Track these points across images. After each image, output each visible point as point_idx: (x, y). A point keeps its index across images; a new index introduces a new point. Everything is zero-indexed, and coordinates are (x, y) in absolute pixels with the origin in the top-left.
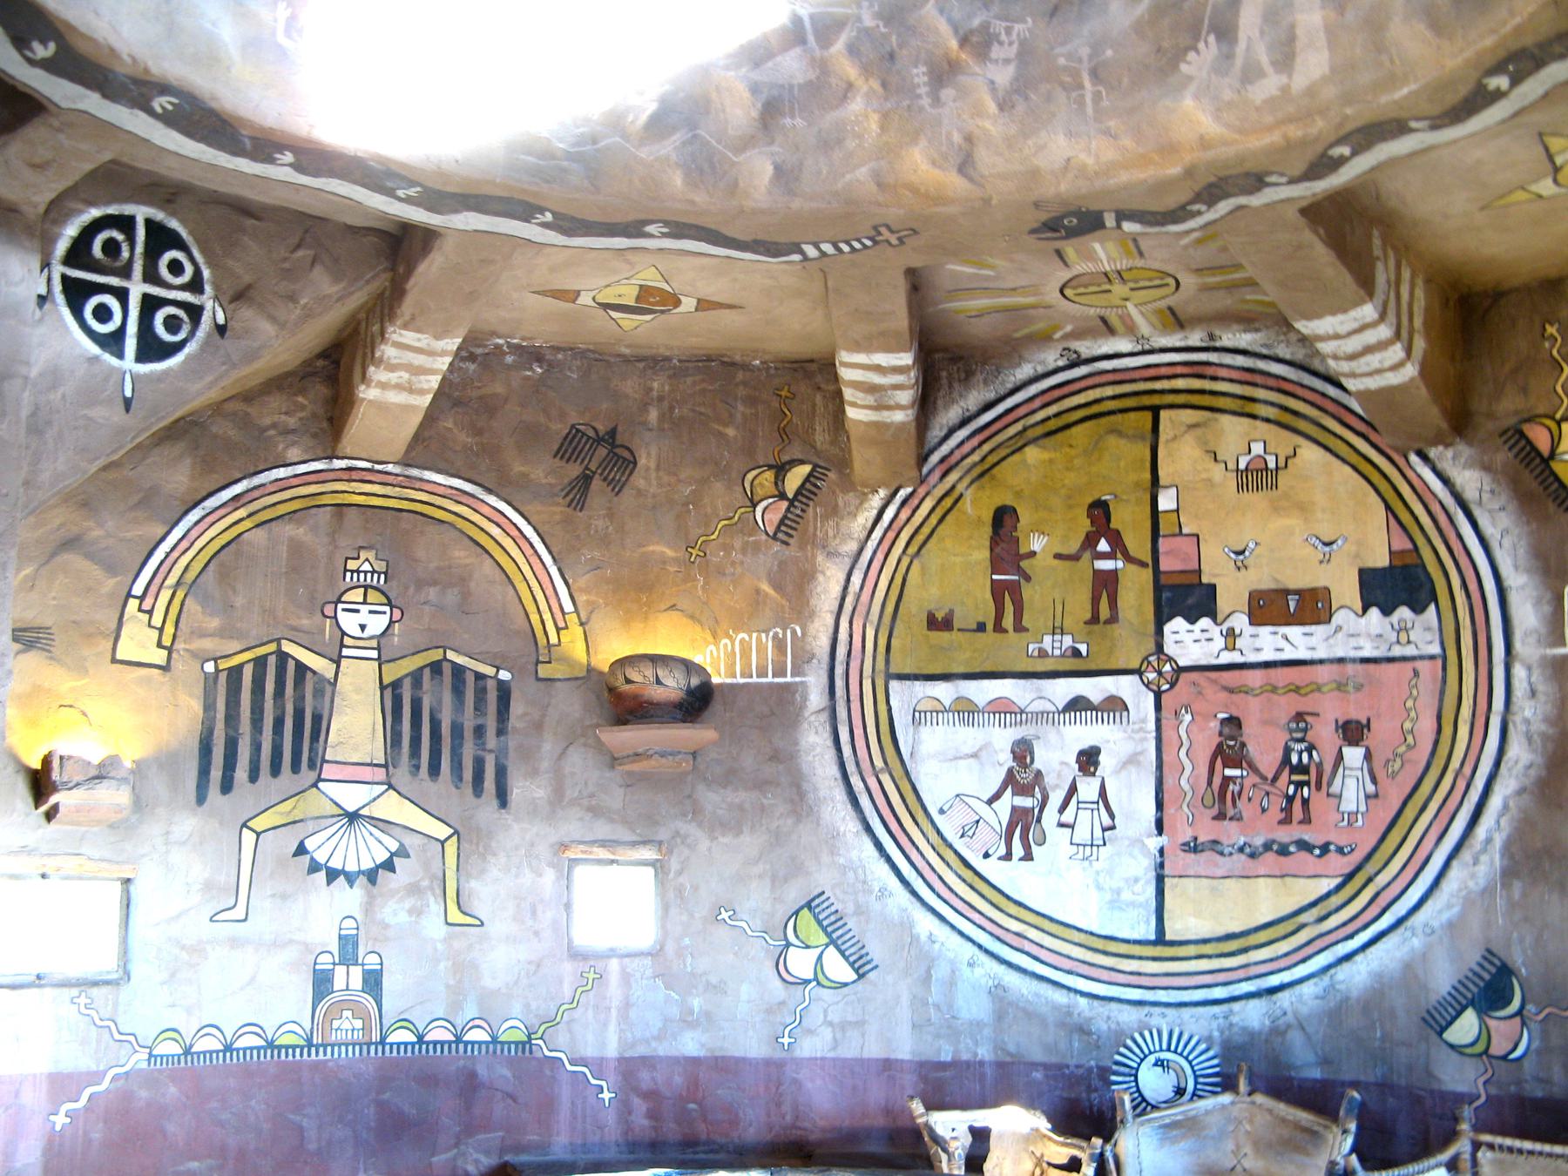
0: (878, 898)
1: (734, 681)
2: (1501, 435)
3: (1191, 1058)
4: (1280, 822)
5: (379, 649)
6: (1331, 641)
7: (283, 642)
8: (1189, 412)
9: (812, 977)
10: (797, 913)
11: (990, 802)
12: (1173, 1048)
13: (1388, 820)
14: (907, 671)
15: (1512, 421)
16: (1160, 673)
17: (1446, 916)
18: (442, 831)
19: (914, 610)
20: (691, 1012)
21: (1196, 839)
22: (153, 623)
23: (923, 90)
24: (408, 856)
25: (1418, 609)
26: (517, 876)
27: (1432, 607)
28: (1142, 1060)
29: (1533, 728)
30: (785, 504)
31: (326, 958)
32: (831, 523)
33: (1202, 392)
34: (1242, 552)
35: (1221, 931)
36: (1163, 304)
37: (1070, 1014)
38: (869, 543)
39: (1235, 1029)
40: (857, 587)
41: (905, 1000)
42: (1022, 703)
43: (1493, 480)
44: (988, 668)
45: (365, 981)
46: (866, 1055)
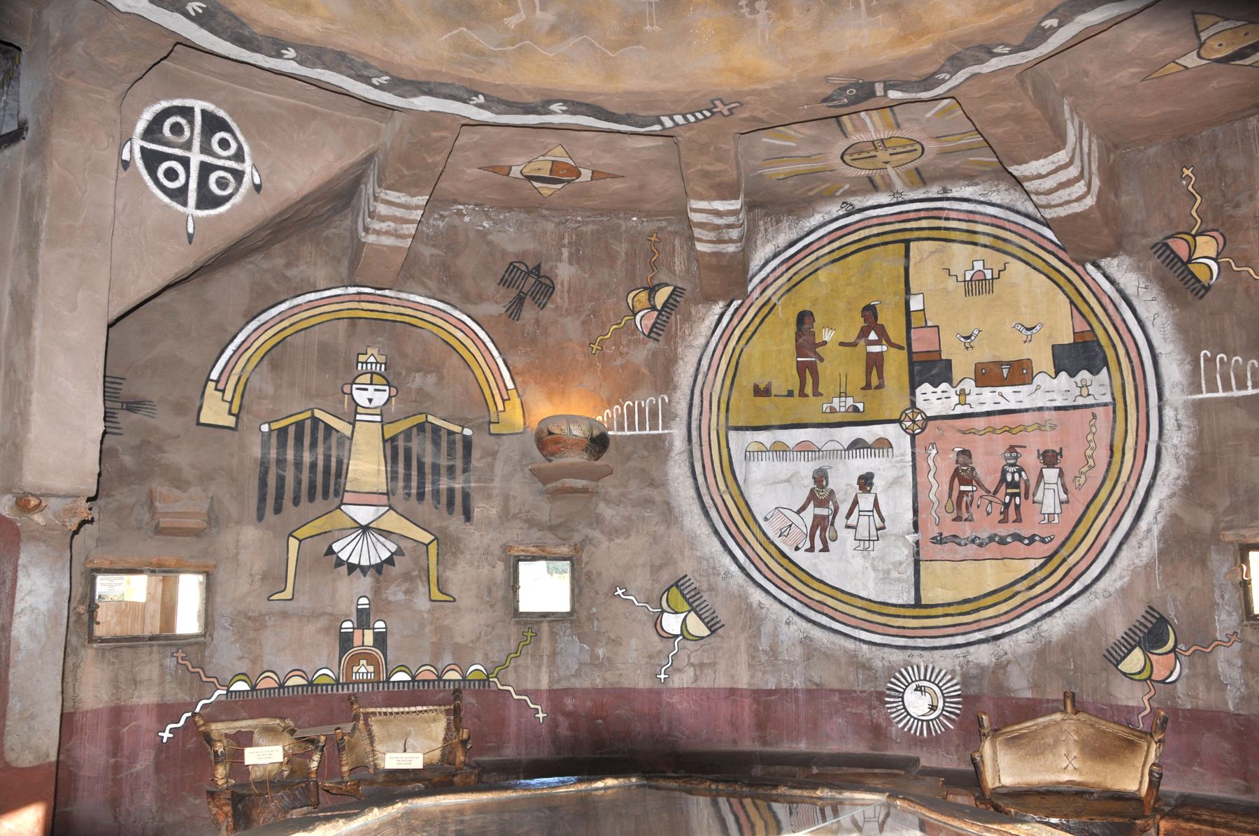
1: (623, 433)
2: (1152, 248)
3: (940, 685)
4: (1000, 522)
5: (381, 415)
6: (1033, 396)
7: (316, 411)
9: (679, 633)
10: (668, 590)
11: (798, 512)
12: (928, 679)
15: (1160, 238)
16: (914, 421)
17: (1118, 585)
18: (426, 537)
19: (745, 383)
20: (598, 658)
21: (941, 534)
22: (225, 398)
24: (403, 555)
25: (1094, 371)
26: (478, 567)
27: (1105, 370)
28: (907, 687)
30: (656, 313)
31: (348, 624)
32: (687, 326)
33: (939, 228)
34: (969, 338)
35: (960, 598)
37: (856, 656)
39: (971, 665)
45: (375, 640)
46: (717, 686)
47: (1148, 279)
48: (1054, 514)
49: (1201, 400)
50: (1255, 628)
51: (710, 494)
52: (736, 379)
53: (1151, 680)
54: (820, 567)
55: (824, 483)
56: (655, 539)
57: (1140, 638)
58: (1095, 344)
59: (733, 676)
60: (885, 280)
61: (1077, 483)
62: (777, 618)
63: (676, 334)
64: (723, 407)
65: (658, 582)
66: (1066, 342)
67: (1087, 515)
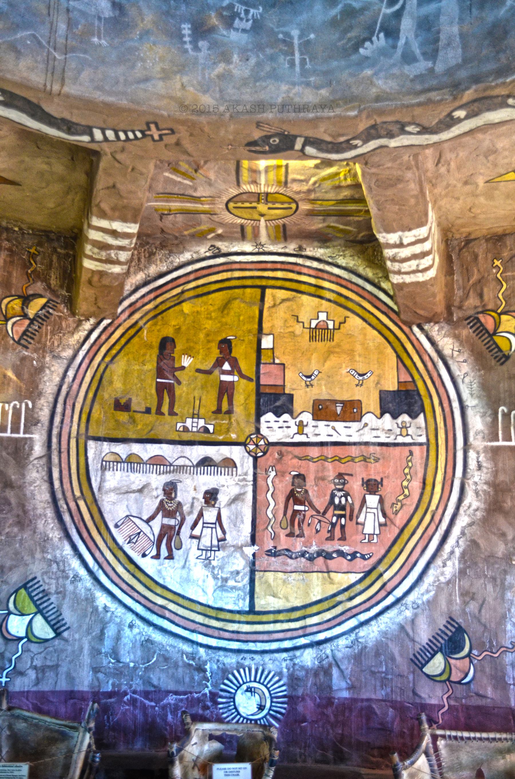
0: (72, 582)
2: (466, 320)
4: (327, 539)
6: (361, 432)
8: (283, 291)
10: (16, 591)
11: (147, 521)
12: (258, 680)
13: (392, 539)
14: (100, 435)
16: (257, 445)
17: (425, 598)
19: (106, 396)
21: (275, 547)
23: (187, 39)
25: (414, 416)
27: (422, 415)
28: (238, 688)
30: (27, 322)
32: (57, 337)
35: (289, 605)
36: (281, 222)
40: (71, 379)
41: (86, 651)
42: (171, 460)
44: (151, 436)
46: (58, 688)
47: (461, 344)
49: (498, 448)
52: (99, 394)
55: (173, 495)
58: (415, 393)
60: (242, 318)
62: (121, 621)
64: (84, 417)
66: (391, 389)
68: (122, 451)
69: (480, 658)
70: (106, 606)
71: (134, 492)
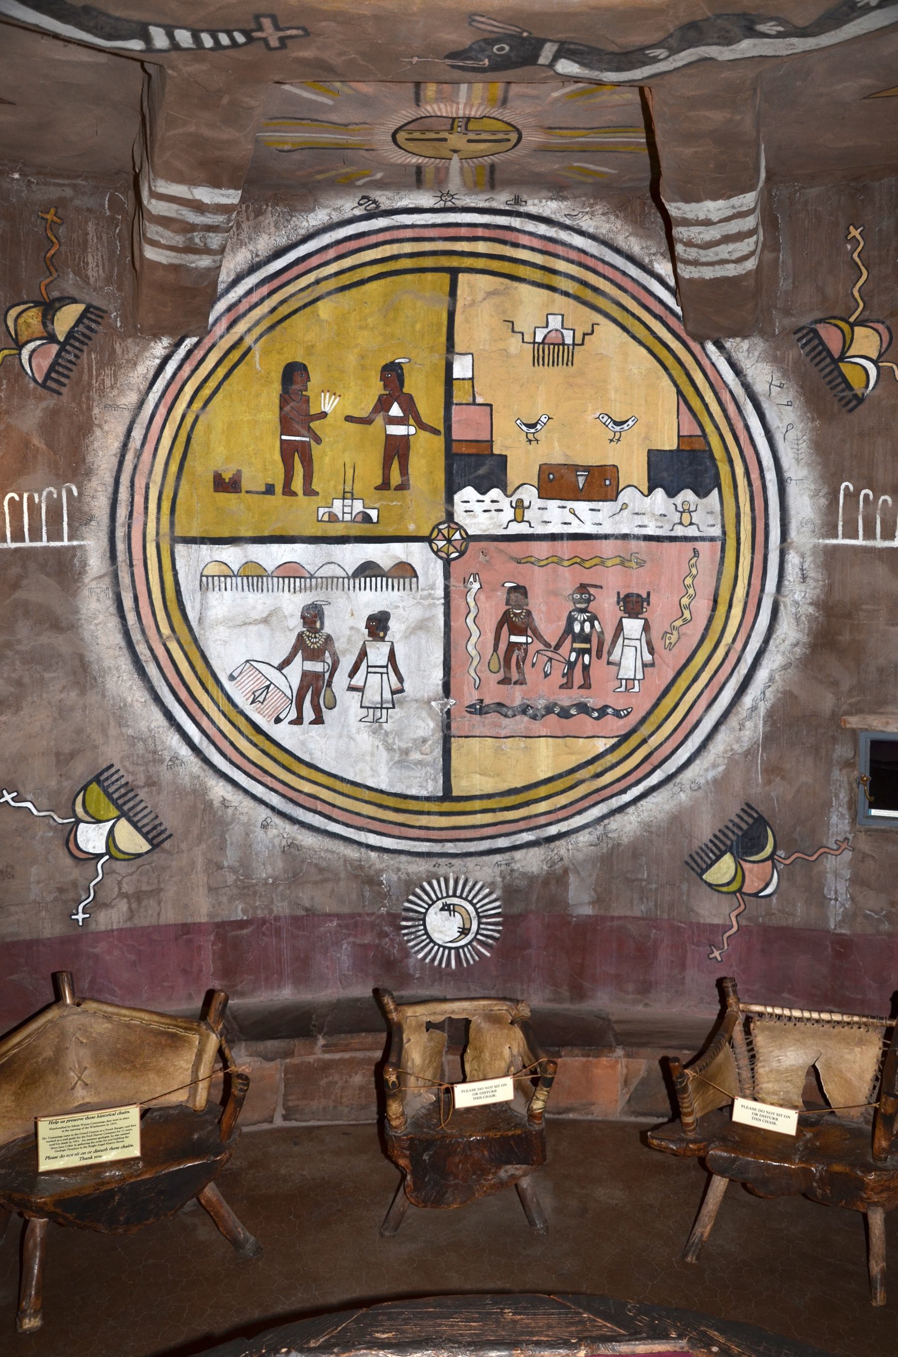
2: (795, 333)
3: (475, 901)
4: (561, 687)
6: (617, 517)
9: (103, 850)
10: (85, 788)
11: (280, 668)
14: (194, 533)
15: (805, 321)
16: (449, 541)
17: (711, 775)
19: (199, 469)
21: (481, 701)
25: (702, 493)
27: (715, 492)
28: (430, 906)
29: (802, 610)
30: (55, 348)
35: (505, 787)
36: (488, 160)
38: (151, 396)
39: (516, 874)
40: (138, 444)
42: (311, 569)
43: (783, 376)
46: (162, 921)
47: (785, 374)
48: (634, 679)
49: (836, 547)
50: (870, 835)
51: (147, 642)
52: (186, 464)
53: (742, 893)
54: (311, 746)
55: (318, 625)
56: (62, 712)
57: (732, 842)
58: (707, 455)
59: (186, 906)
60: (418, 326)
61: (668, 642)
62: (249, 820)
63: (90, 385)
65: (69, 778)
66: (667, 448)
67: (677, 684)
68: (231, 559)
69: (788, 862)
70: (224, 799)
71: (256, 622)
